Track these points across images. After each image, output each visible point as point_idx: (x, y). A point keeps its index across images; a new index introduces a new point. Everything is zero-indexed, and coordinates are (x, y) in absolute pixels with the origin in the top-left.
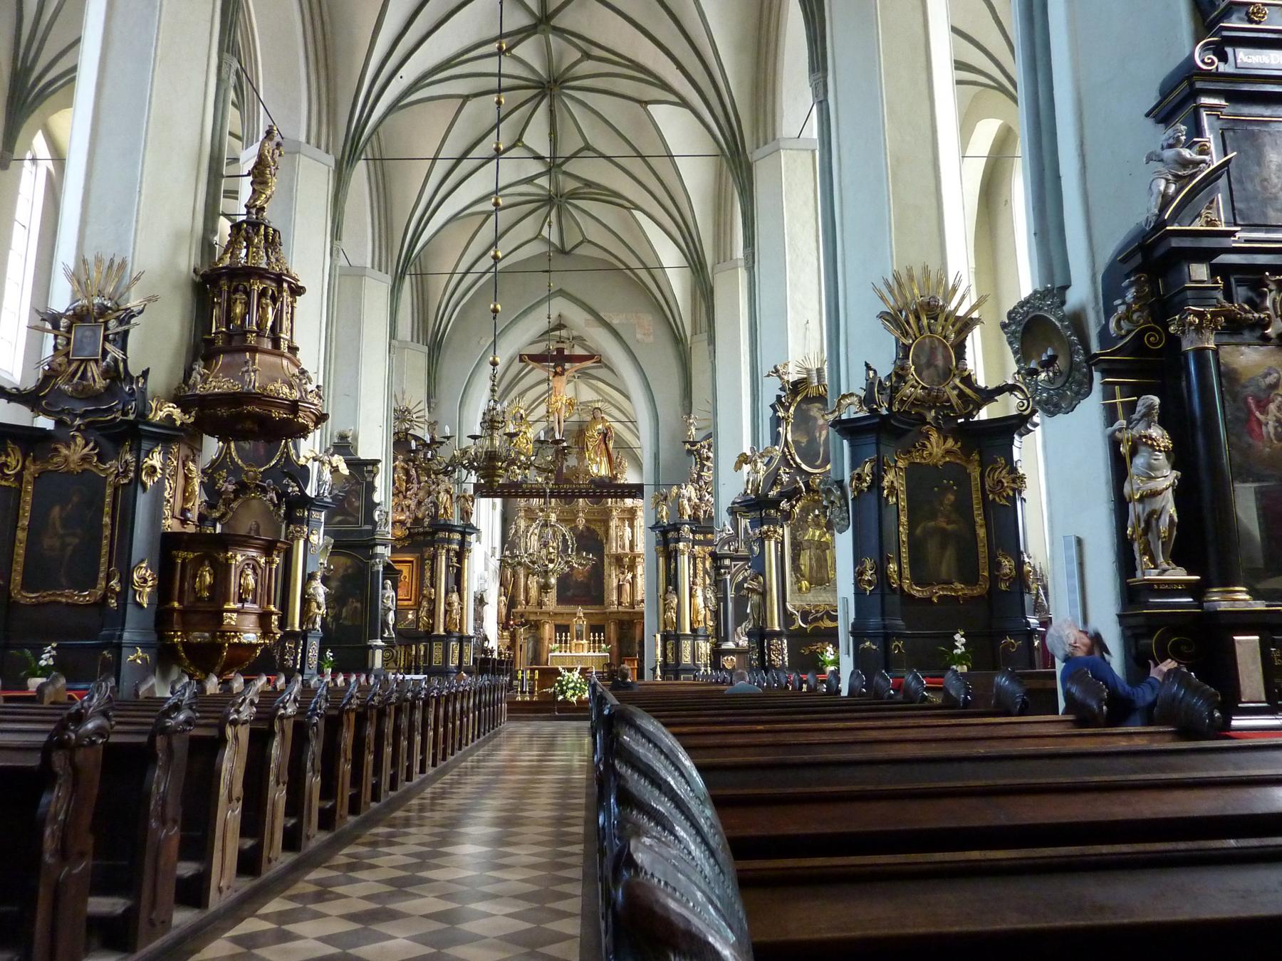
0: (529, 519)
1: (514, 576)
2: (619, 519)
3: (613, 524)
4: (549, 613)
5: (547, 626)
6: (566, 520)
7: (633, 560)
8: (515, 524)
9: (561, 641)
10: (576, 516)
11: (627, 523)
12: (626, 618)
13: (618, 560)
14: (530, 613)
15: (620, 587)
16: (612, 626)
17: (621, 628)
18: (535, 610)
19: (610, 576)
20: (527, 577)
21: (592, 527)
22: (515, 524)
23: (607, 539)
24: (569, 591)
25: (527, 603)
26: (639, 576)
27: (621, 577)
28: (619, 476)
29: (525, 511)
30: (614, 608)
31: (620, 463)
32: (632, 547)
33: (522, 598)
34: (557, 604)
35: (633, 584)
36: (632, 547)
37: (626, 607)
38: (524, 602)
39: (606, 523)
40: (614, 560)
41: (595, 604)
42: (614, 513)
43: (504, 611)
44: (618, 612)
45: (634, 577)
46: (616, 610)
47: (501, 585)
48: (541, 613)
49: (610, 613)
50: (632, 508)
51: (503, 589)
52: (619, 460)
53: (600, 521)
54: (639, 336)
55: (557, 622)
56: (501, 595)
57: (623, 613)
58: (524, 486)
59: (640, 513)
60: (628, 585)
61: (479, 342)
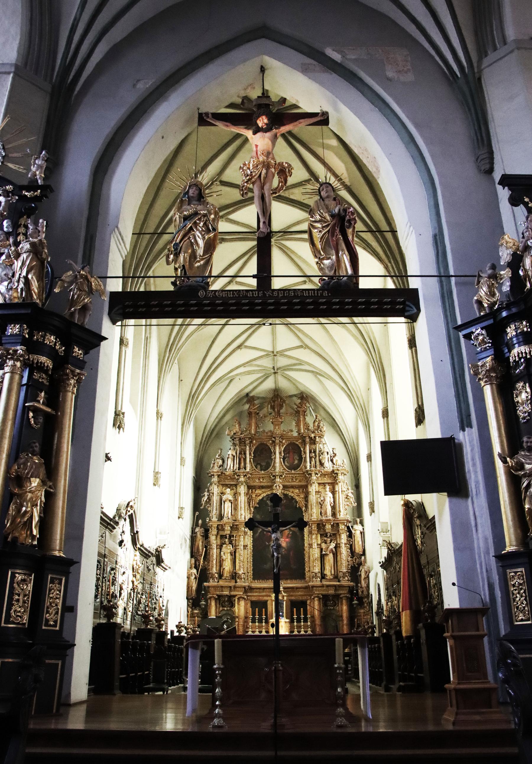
0: (223, 485)
1: (206, 547)
2: (319, 484)
3: (313, 488)
4: (245, 588)
5: (242, 603)
6: (262, 487)
7: (336, 526)
8: (208, 491)
9: (260, 621)
10: (273, 481)
11: (328, 487)
12: (331, 592)
13: (320, 525)
14: (222, 587)
15: (322, 557)
16: (316, 603)
17: (325, 605)
18: (227, 584)
19: (311, 546)
20: (220, 547)
21: (290, 494)
22: (208, 491)
23: (306, 506)
24: (266, 564)
25: (221, 576)
26: (343, 545)
27: (324, 546)
28: (318, 439)
29: (219, 476)
30: (317, 582)
31: (319, 427)
32: (334, 514)
33: (214, 570)
34: (254, 579)
35: (336, 553)
36: (334, 514)
37: (330, 580)
38: (217, 575)
39: (305, 489)
40: (314, 527)
41: (296, 579)
42: (314, 477)
43: (194, 586)
44: (323, 586)
45: (337, 547)
46: (319, 583)
47: (192, 556)
48: (235, 587)
49: (313, 587)
50: (333, 471)
51: (193, 560)
52: (316, 424)
53: (299, 487)
54: (390, 74)
55: (254, 599)
56: (191, 568)
57: (328, 586)
58: (201, 293)
59: (341, 477)
60: (331, 556)
61: (134, 86)
